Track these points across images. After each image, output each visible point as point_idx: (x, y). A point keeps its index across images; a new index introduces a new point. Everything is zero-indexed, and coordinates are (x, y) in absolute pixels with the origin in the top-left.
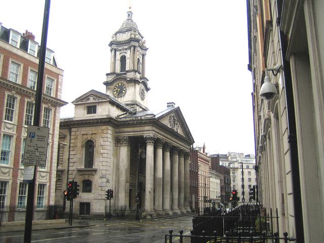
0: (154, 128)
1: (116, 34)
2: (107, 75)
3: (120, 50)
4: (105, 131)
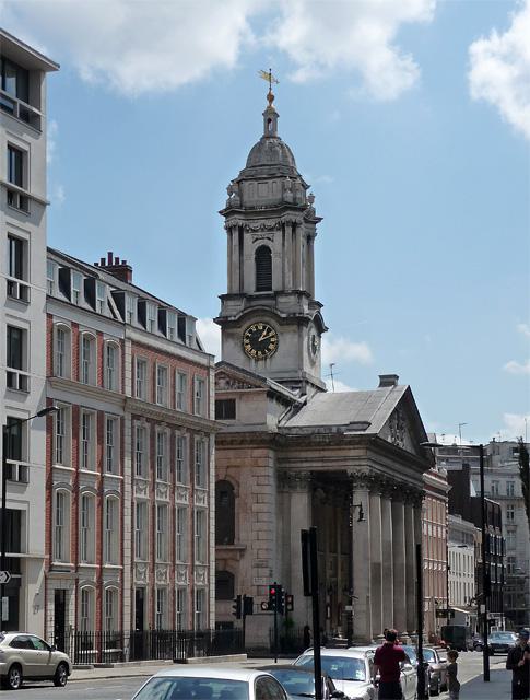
1: (239, 182)
3: (254, 231)
4: (260, 462)
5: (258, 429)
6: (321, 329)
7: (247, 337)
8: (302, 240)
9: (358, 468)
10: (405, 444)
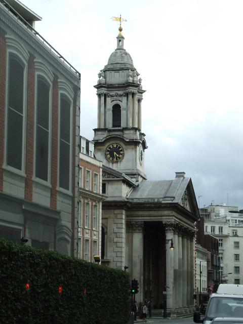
0: (174, 213)
1: (105, 71)
2: (95, 130)
3: (112, 96)
4: (119, 216)
5: (117, 199)
6: (144, 147)
7: (108, 151)
8: (136, 102)
9: (169, 220)
10: (188, 208)
